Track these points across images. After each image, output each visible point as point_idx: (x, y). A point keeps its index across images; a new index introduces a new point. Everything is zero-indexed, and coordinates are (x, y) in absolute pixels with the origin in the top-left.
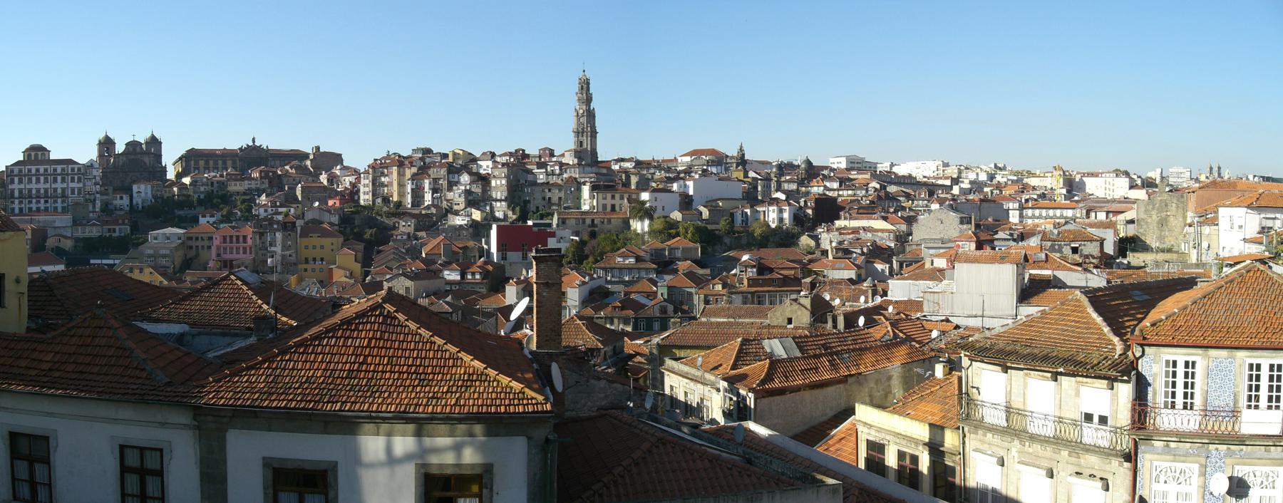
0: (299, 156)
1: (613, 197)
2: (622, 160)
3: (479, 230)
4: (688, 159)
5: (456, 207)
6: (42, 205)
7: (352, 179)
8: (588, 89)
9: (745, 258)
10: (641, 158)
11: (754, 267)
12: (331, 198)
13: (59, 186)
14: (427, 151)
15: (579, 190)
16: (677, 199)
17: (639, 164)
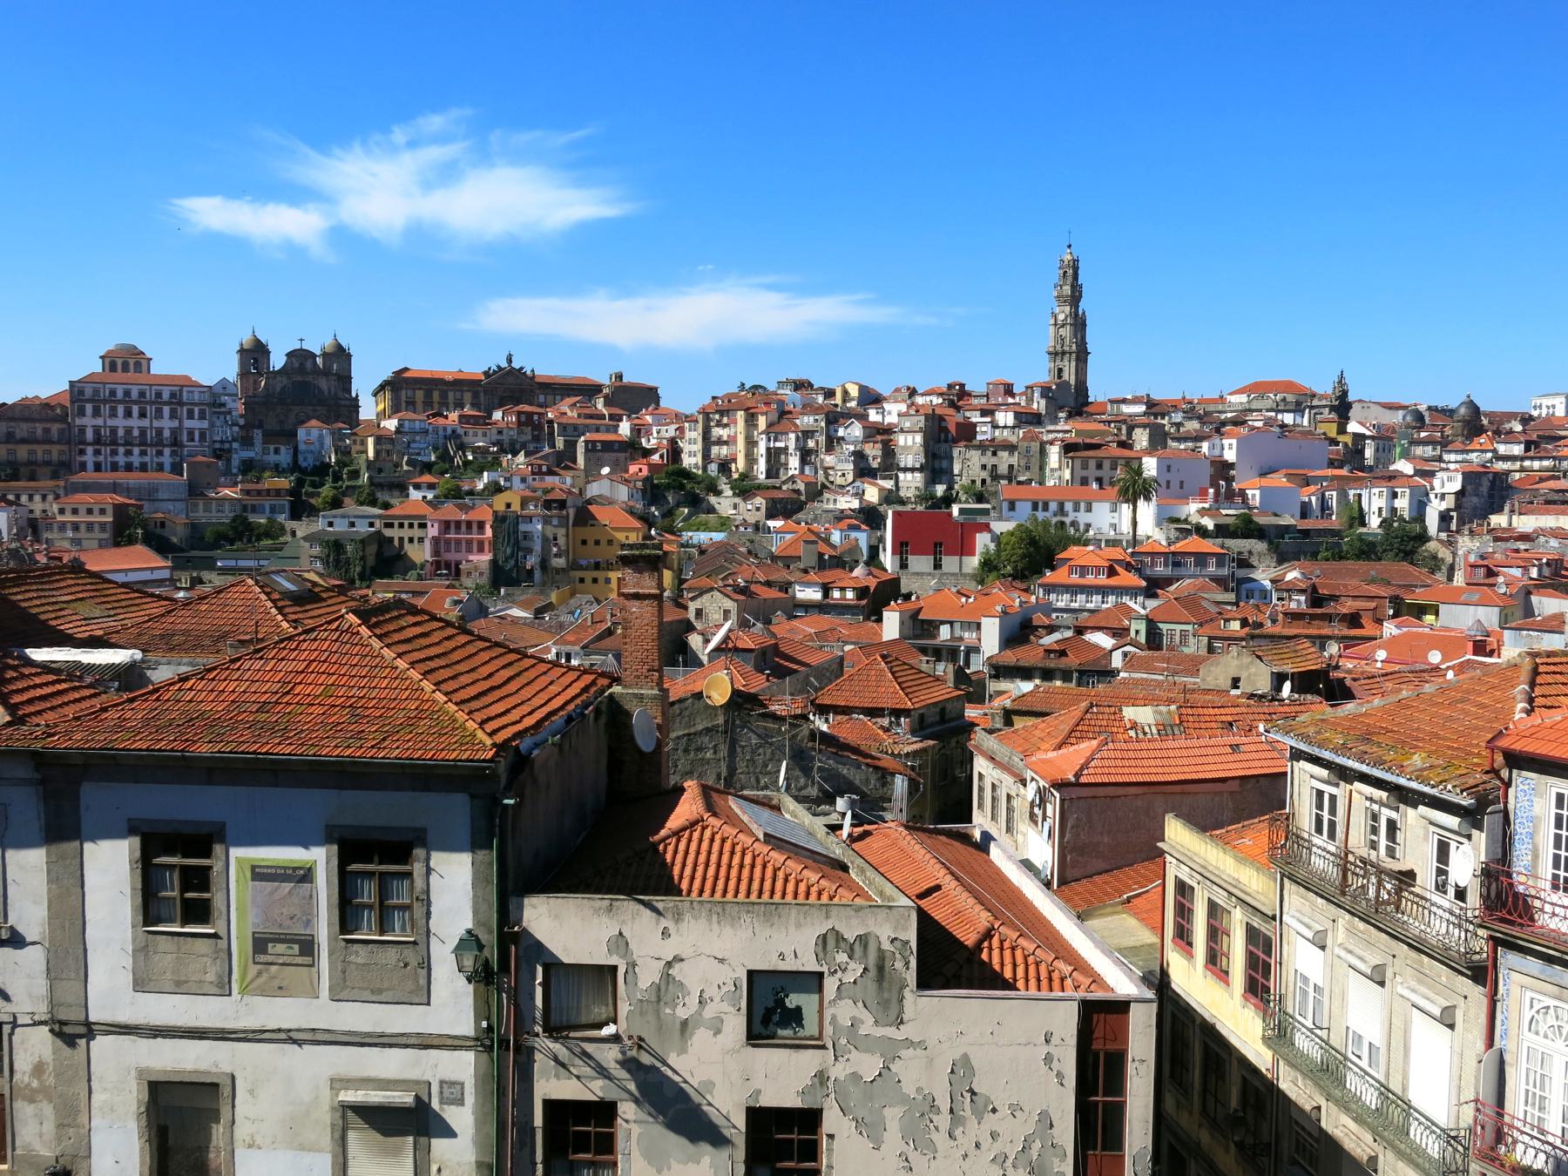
0: (588, 390)
1: (1099, 466)
2: (1124, 401)
3: (870, 517)
4: (1243, 398)
5: (840, 481)
6: (136, 460)
7: (671, 431)
8: (1076, 276)
9: (1290, 576)
10: (1157, 396)
11: (1302, 591)
12: (633, 459)
13: (167, 424)
14: (799, 385)
15: (1043, 453)
16: (1208, 471)
17: (1154, 407)
